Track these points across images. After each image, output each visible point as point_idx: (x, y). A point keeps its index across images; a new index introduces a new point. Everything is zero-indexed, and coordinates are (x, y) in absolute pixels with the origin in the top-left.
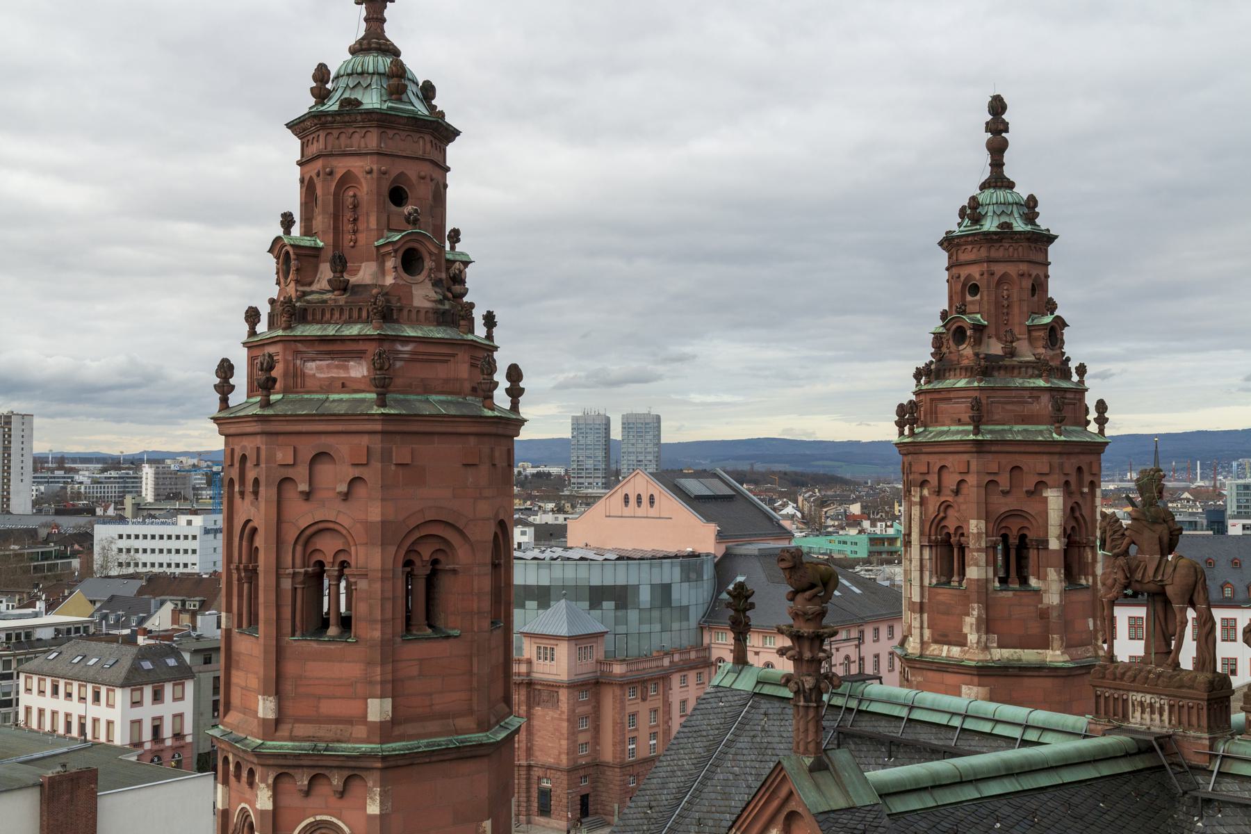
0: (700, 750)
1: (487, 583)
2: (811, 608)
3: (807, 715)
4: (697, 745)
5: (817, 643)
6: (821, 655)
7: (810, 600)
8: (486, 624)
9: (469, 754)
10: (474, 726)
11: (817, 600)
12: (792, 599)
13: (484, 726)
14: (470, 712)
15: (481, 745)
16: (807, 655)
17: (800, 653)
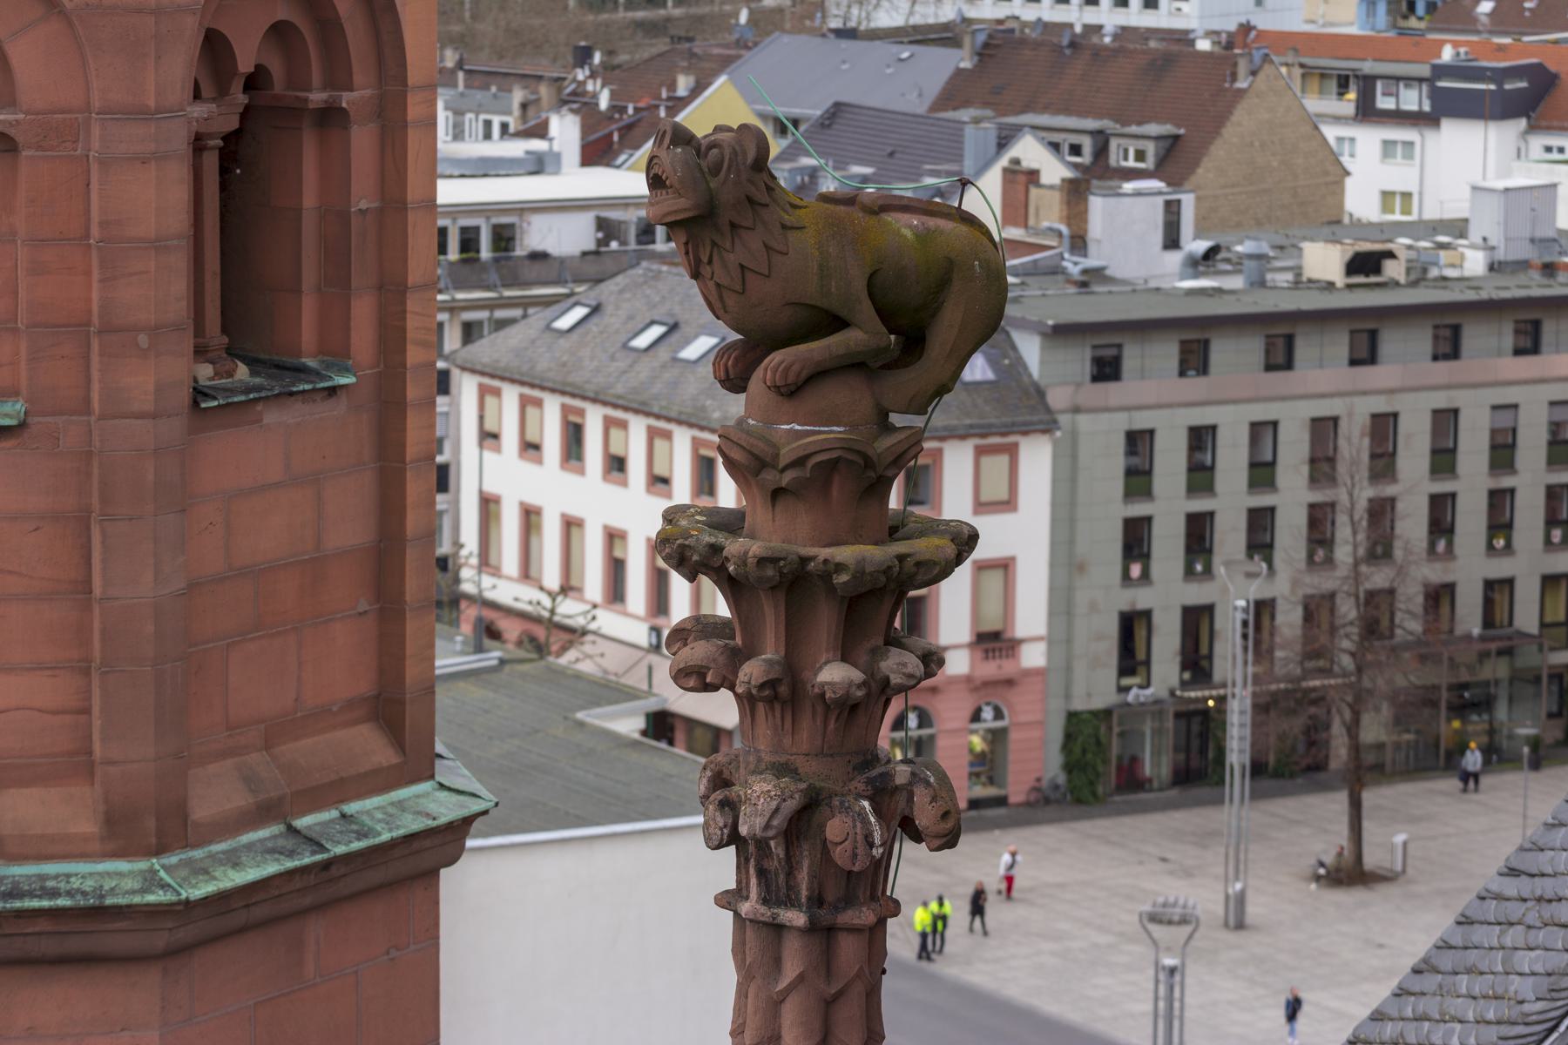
0: (1520, 986)
1: (154, 197)
2: (797, 433)
3: (777, 962)
4: (1525, 961)
5: (825, 621)
6: (834, 675)
7: (792, 390)
8: (156, 376)
9: (50, 947)
10: (87, 825)
11: (848, 395)
12: (734, 382)
13: (155, 825)
14: (78, 764)
15: (99, 913)
16: (752, 672)
17: (736, 657)
